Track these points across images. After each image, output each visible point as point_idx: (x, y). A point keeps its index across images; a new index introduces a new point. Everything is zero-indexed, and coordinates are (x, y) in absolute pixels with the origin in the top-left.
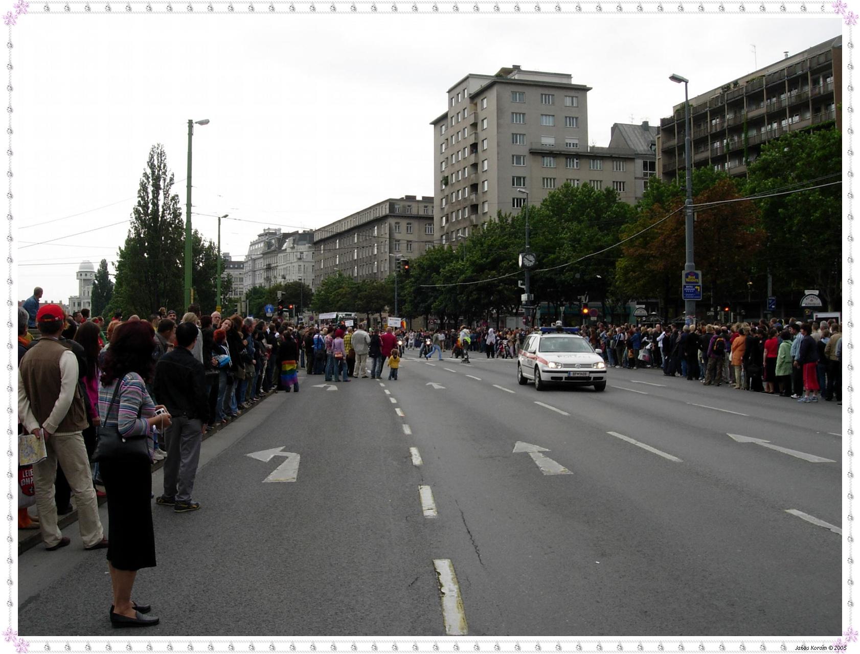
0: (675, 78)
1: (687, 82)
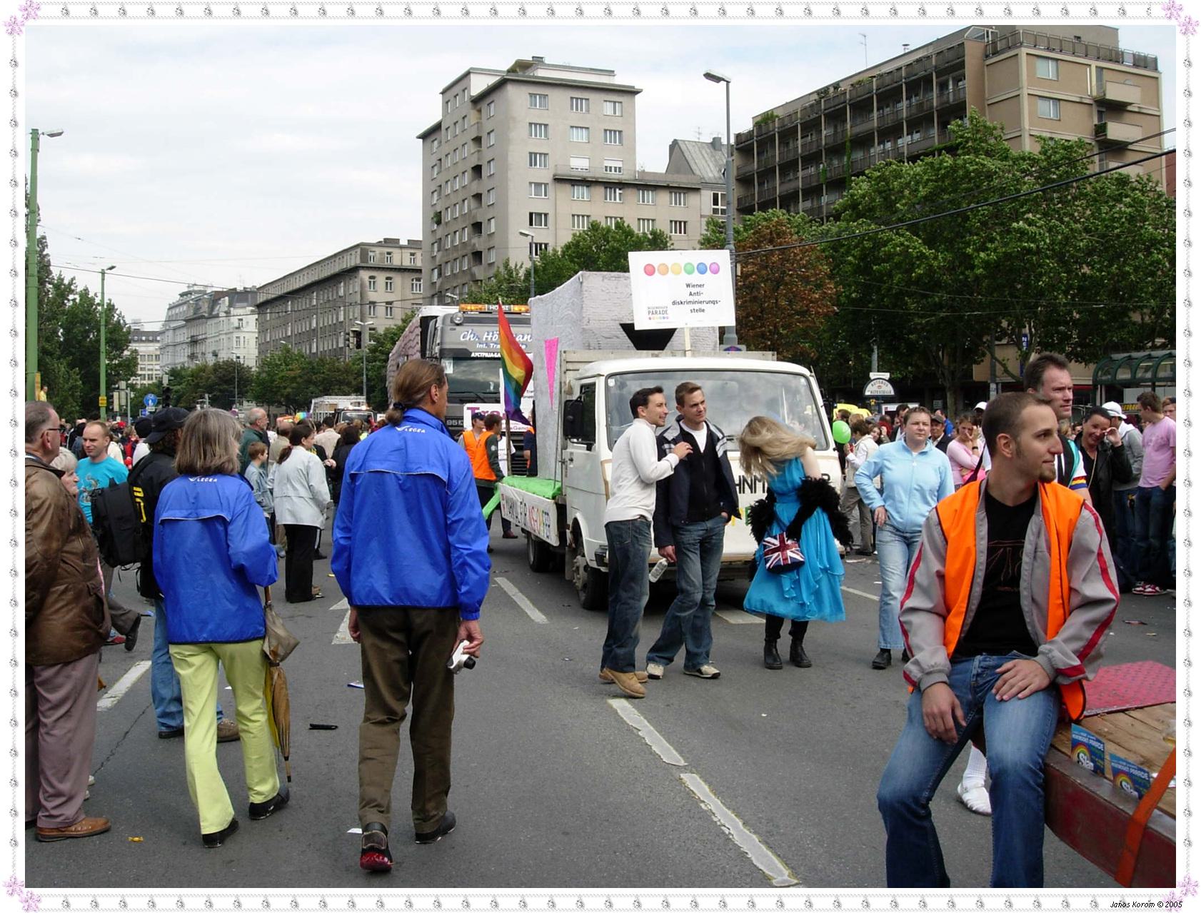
0: (709, 76)
1: (728, 82)
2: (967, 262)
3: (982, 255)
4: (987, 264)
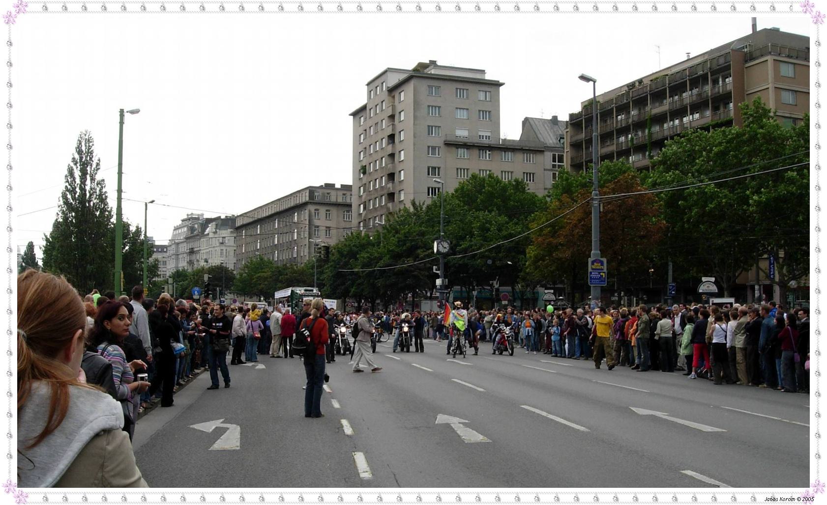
0: (583, 78)
1: (594, 82)
2: (745, 200)
3: (755, 197)
4: (758, 203)
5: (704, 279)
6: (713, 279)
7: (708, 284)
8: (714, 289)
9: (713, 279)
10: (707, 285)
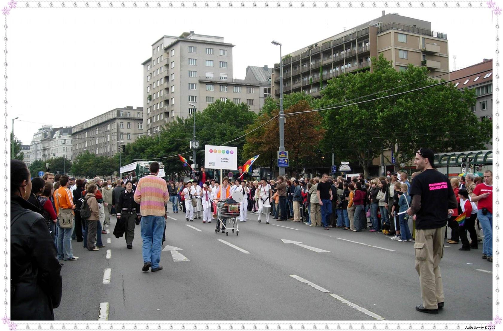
2: (374, 116)
4: (382, 118)
5: (342, 163)
6: (348, 163)
7: (345, 166)
8: (349, 168)
9: (348, 163)
10: (344, 166)
